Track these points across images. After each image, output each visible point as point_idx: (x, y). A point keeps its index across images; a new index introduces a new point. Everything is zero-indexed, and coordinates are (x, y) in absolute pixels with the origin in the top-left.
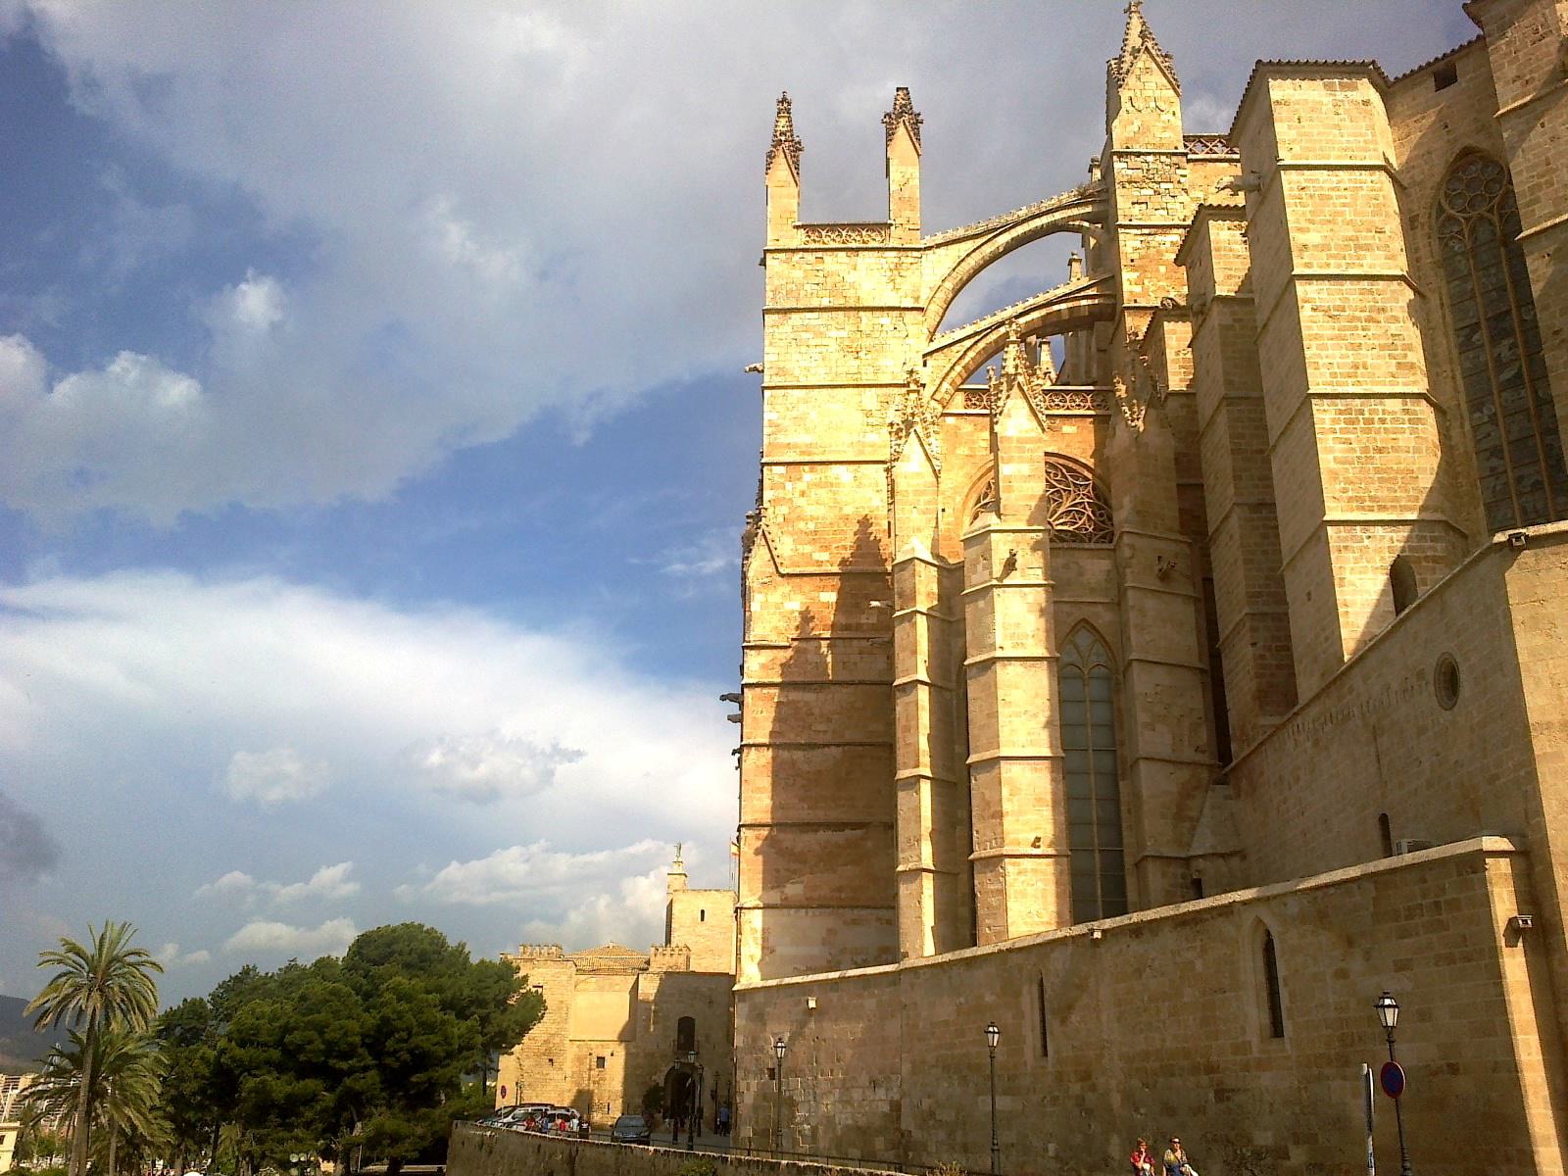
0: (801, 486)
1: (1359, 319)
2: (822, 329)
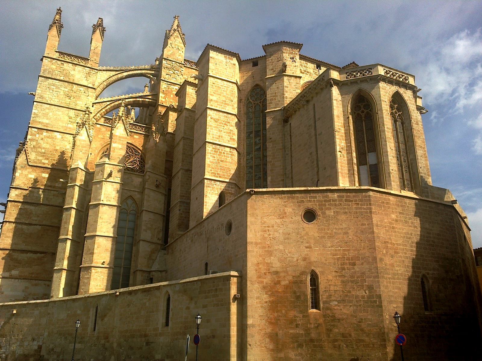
0: (42, 136)
1: (222, 124)
2: (59, 86)
